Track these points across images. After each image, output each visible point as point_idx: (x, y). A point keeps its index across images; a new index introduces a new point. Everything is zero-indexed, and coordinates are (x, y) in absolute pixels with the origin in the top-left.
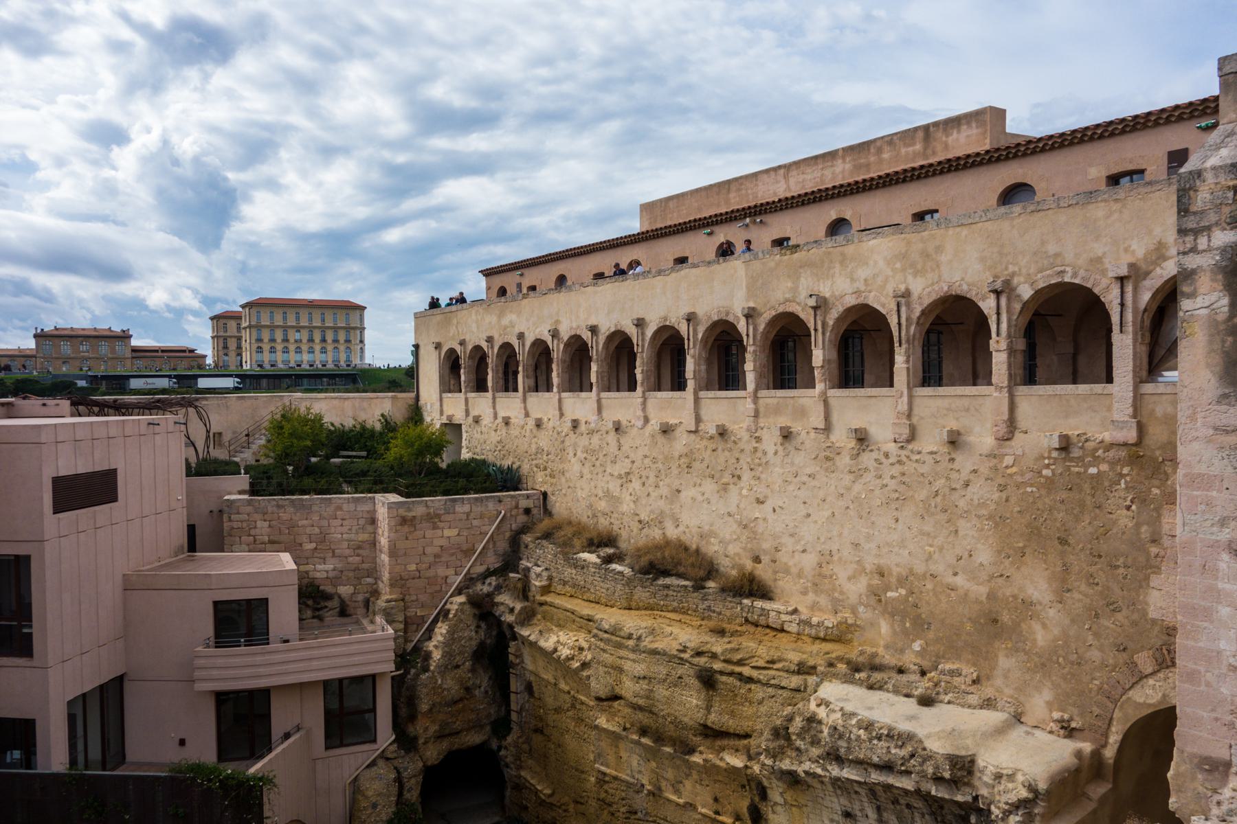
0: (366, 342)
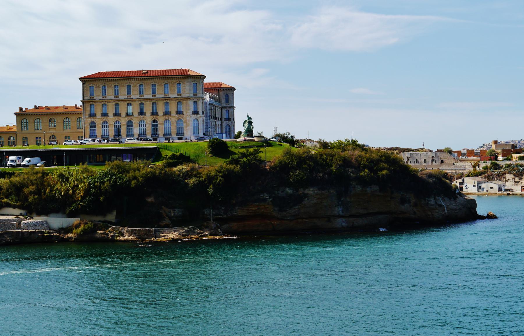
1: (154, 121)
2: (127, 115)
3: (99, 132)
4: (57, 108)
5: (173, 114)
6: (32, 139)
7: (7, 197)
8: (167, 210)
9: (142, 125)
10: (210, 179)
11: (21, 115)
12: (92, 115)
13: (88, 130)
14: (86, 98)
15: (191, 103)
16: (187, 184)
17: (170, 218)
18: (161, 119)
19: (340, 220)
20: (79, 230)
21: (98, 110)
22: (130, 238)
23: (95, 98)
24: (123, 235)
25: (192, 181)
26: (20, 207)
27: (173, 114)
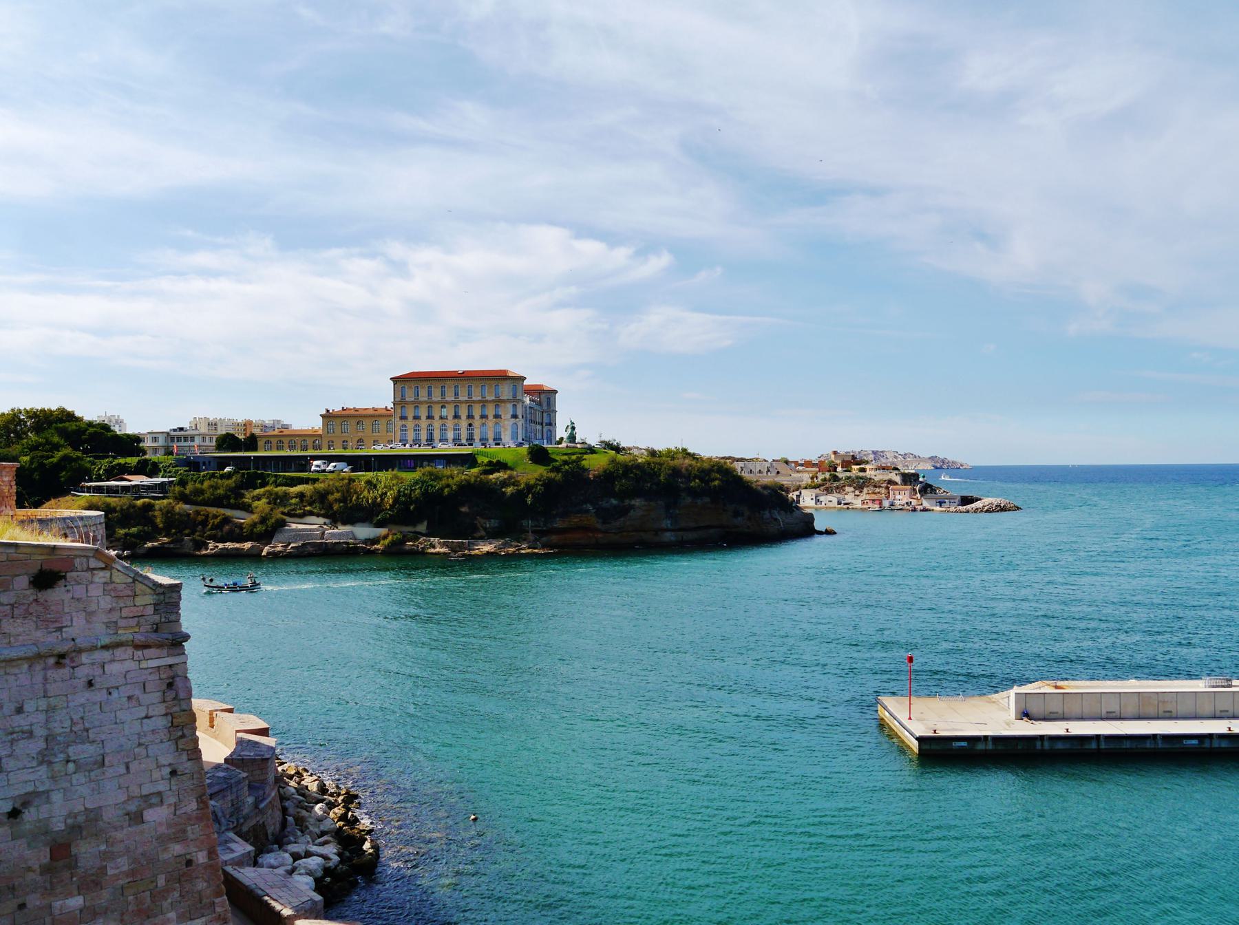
1: (470, 425)
2: (441, 418)
3: (411, 436)
5: (491, 417)
6: (338, 443)
7: (310, 505)
8: (482, 521)
9: (456, 429)
10: (529, 488)
11: (328, 417)
12: (403, 418)
13: (399, 433)
15: (510, 406)
16: (504, 493)
17: (485, 529)
18: (477, 423)
19: (668, 534)
20: (387, 541)
21: (410, 413)
22: (442, 550)
24: (434, 547)
25: (509, 490)
26: (324, 516)
27: (491, 417)
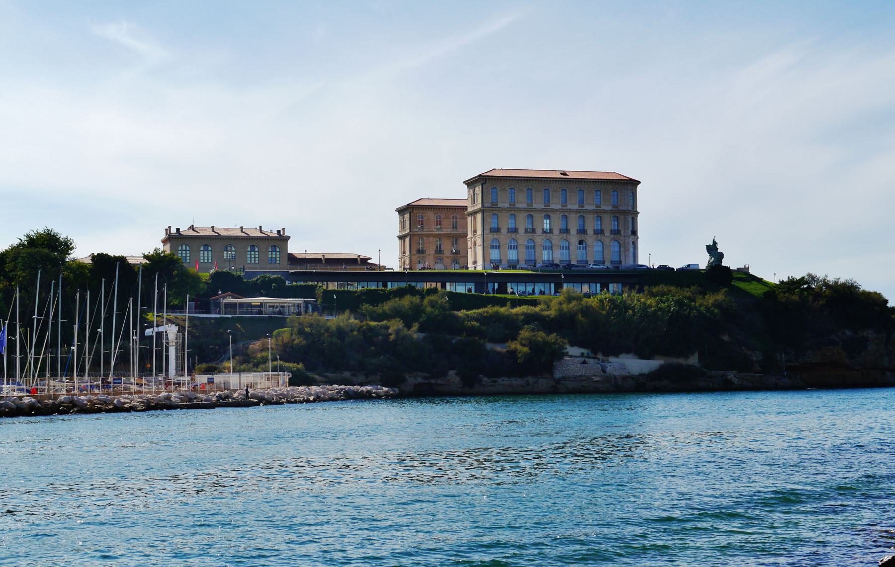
0: (639, 233)
4: (226, 230)
14: (486, 205)
23: (500, 205)
